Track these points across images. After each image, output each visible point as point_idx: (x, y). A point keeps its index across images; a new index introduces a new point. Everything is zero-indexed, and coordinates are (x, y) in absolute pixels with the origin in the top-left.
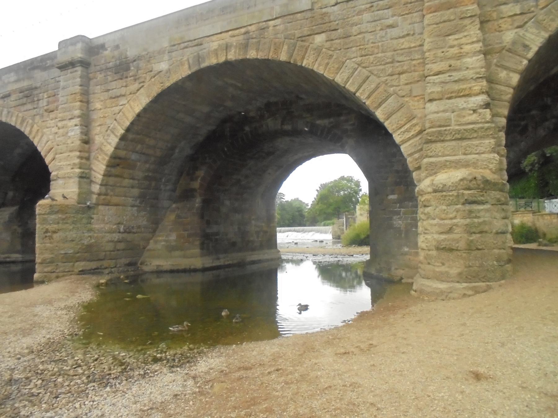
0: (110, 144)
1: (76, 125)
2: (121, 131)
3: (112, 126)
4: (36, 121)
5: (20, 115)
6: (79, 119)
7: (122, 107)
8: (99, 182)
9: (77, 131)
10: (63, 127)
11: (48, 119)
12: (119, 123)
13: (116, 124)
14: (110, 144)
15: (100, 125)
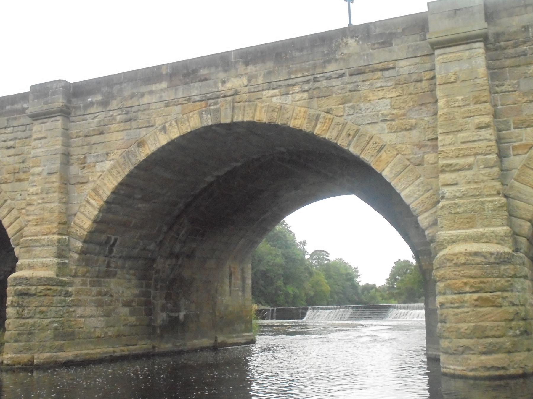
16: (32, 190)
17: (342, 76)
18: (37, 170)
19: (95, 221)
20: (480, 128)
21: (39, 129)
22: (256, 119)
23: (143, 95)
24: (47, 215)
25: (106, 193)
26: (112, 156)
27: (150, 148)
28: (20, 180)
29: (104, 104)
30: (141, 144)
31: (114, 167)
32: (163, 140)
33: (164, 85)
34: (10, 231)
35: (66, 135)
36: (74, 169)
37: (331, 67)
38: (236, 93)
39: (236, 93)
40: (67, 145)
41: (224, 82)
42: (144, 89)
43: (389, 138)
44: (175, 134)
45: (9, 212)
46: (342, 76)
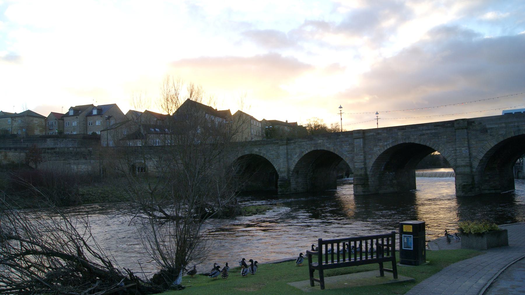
0: (480, 156)
1: (466, 149)
2: (485, 152)
3: (481, 150)
4: (440, 145)
5: (431, 142)
6: (467, 147)
7: (485, 144)
8: (475, 168)
9: (467, 151)
10: (460, 150)
11: (447, 145)
12: (484, 149)
13: (483, 150)
14: (480, 156)
15: (475, 149)
16: (281, 161)
17: (339, 142)
19: (294, 168)
20: (361, 155)
21: (281, 147)
22: (324, 149)
23: (302, 142)
24: (284, 166)
26: (297, 154)
27: (305, 153)
28: (278, 158)
29: (294, 143)
30: (303, 152)
31: (298, 157)
32: (307, 152)
35: (287, 149)
36: (289, 157)
37: (338, 140)
39: (320, 143)
40: (287, 151)
42: (303, 140)
43: (348, 155)
44: (309, 151)
45: (276, 165)
46: (339, 142)
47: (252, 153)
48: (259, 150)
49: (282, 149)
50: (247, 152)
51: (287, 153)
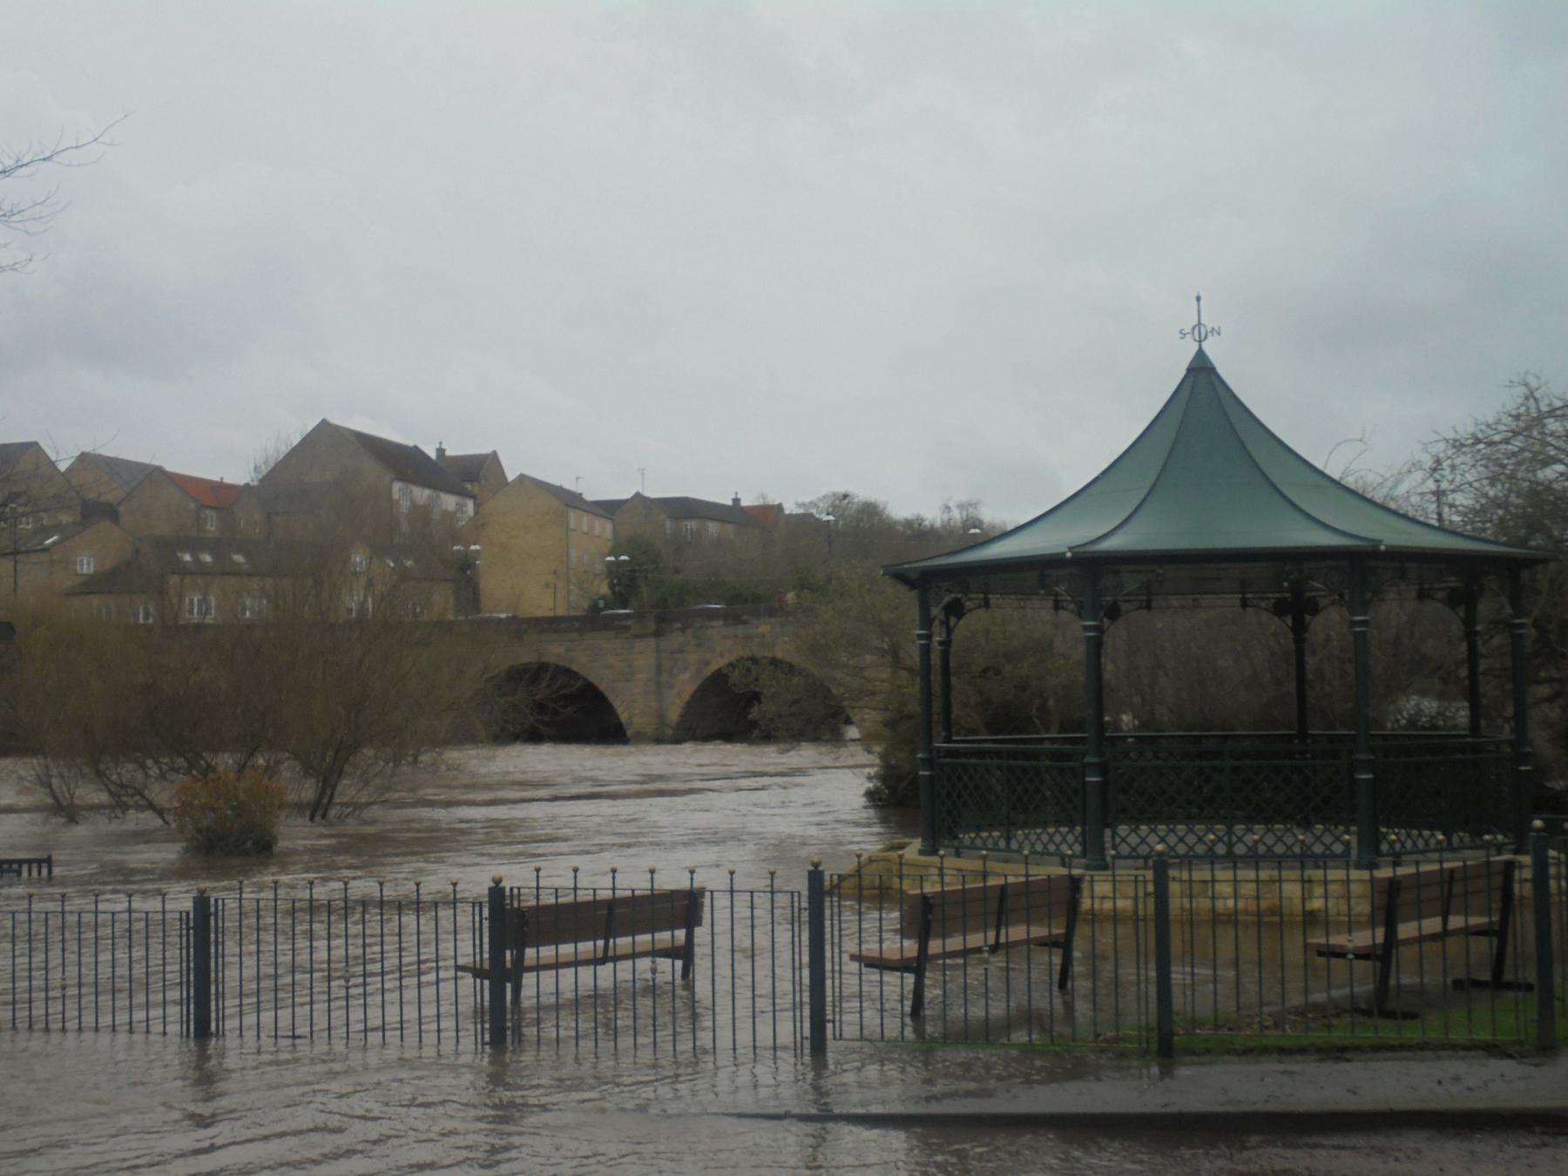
18: (640, 676)
21: (640, 645)
25: (687, 697)
29: (683, 630)
30: (708, 663)
33: (720, 623)
34: (624, 718)
36: (665, 677)
38: (763, 636)
41: (757, 627)
47: (544, 660)
48: (568, 650)
49: (644, 654)
50: (526, 657)
51: (659, 667)
